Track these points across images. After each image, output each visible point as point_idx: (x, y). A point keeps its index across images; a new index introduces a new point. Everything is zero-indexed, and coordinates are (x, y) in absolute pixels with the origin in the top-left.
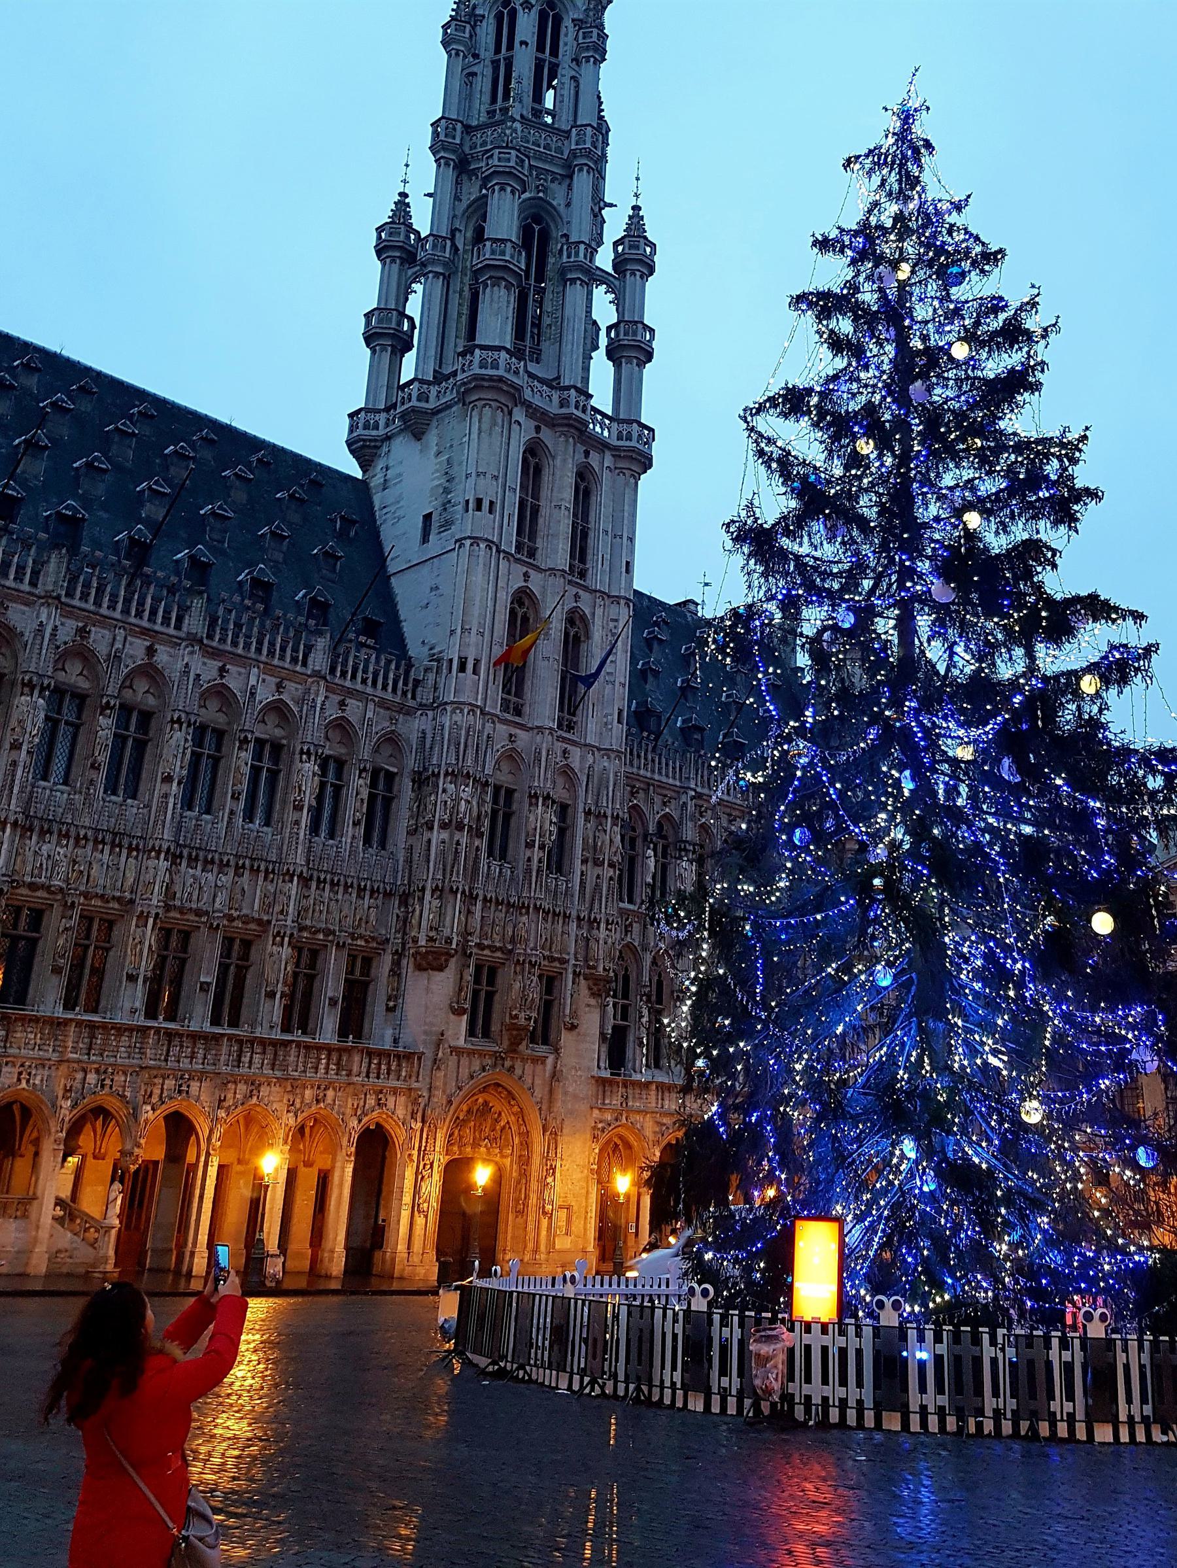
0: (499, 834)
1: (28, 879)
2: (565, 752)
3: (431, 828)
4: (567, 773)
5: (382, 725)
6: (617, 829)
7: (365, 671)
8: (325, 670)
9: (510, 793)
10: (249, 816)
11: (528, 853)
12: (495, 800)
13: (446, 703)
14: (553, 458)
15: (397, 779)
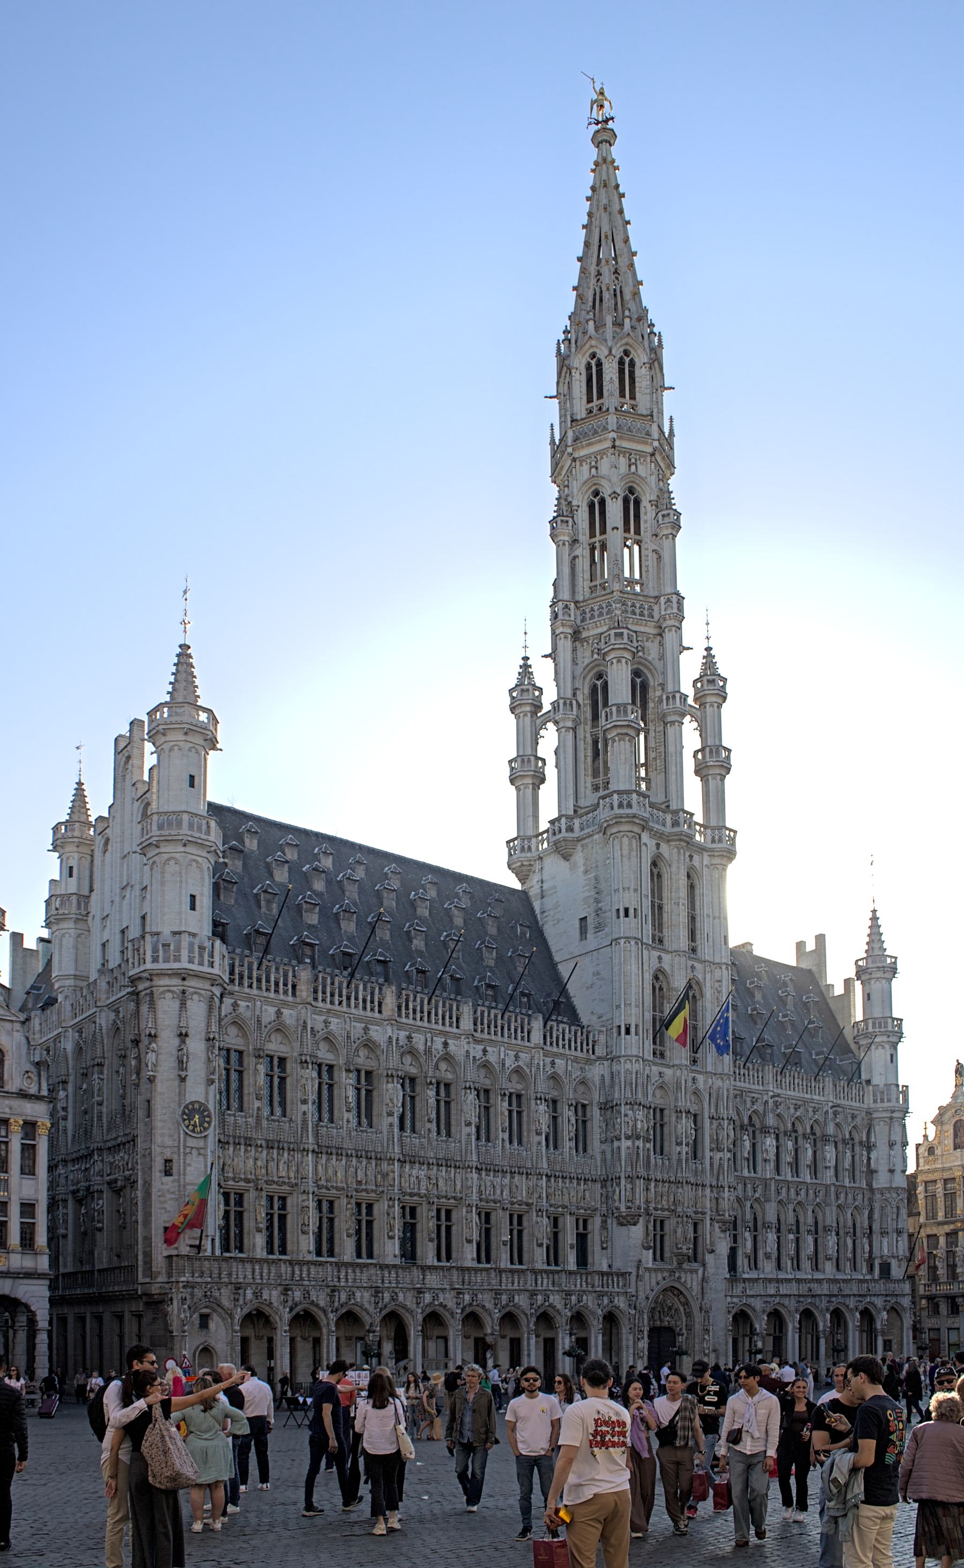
0: (658, 1138)
1: (408, 1191)
2: (694, 1079)
3: (619, 1139)
4: (696, 1093)
5: (577, 1074)
6: (731, 1127)
7: (563, 1040)
8: (542, 1041)
9: (662, 1110)
10: (511, 1142)
11: (678, 1149)
12: (654, 1119)
13: (619, 1057)
14: (670, 866)
15: (588, 1108)
